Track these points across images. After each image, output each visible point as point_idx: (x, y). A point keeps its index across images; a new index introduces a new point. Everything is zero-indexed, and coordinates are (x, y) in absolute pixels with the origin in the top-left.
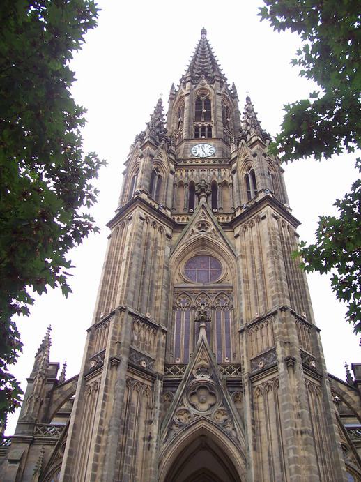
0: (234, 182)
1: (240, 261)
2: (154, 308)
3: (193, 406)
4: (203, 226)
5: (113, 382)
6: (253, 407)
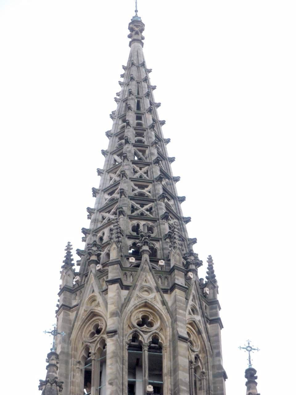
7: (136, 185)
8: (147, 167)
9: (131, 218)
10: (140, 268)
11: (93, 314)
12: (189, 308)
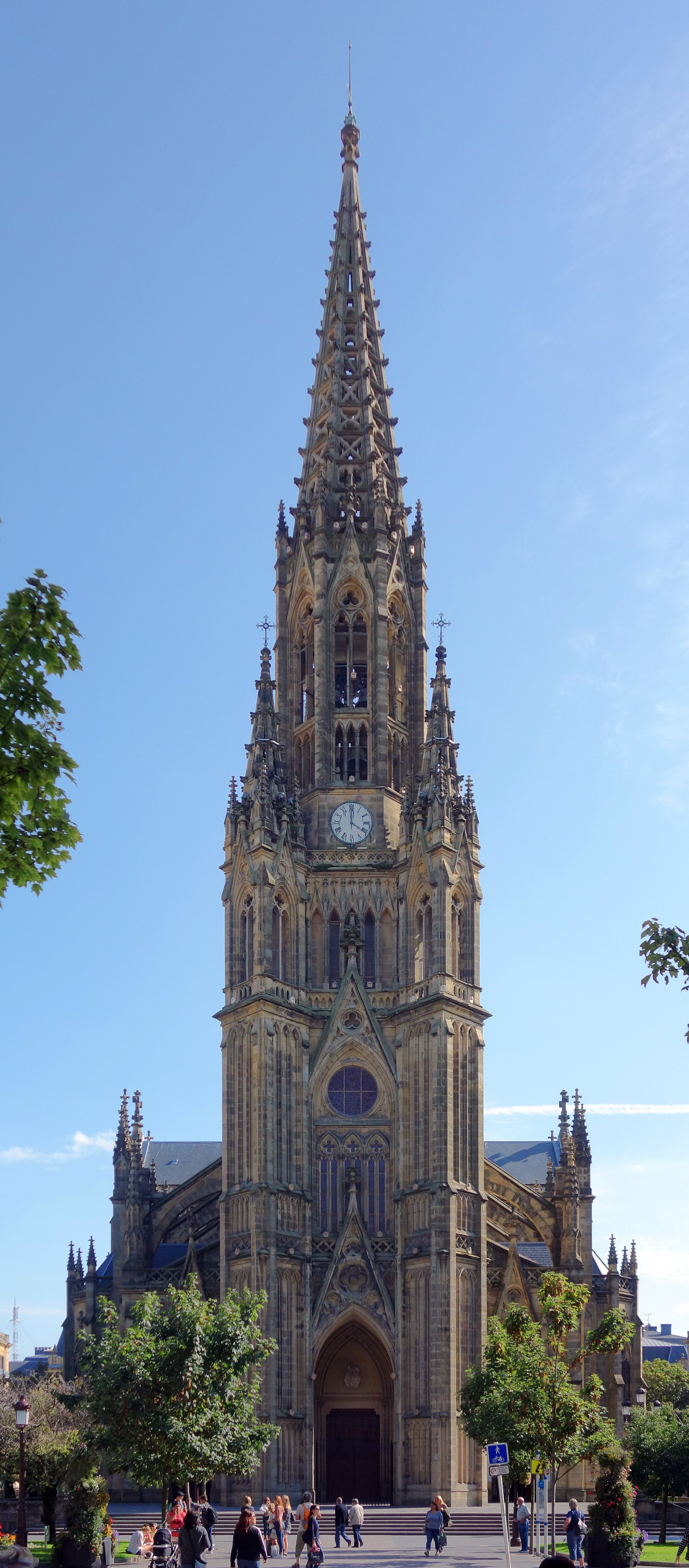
0: (401, 916)
1: (400, 1091)
2: (294, 1168)
3: (344, 1289)
4: (352, 1019)
5: (264, 1279)
6: (405, 1293)
7: (345, 412)
8: (356, 383)
9: (339, 463)
10: (344, 534)
11: (303, 593)
12: (393, 575)
